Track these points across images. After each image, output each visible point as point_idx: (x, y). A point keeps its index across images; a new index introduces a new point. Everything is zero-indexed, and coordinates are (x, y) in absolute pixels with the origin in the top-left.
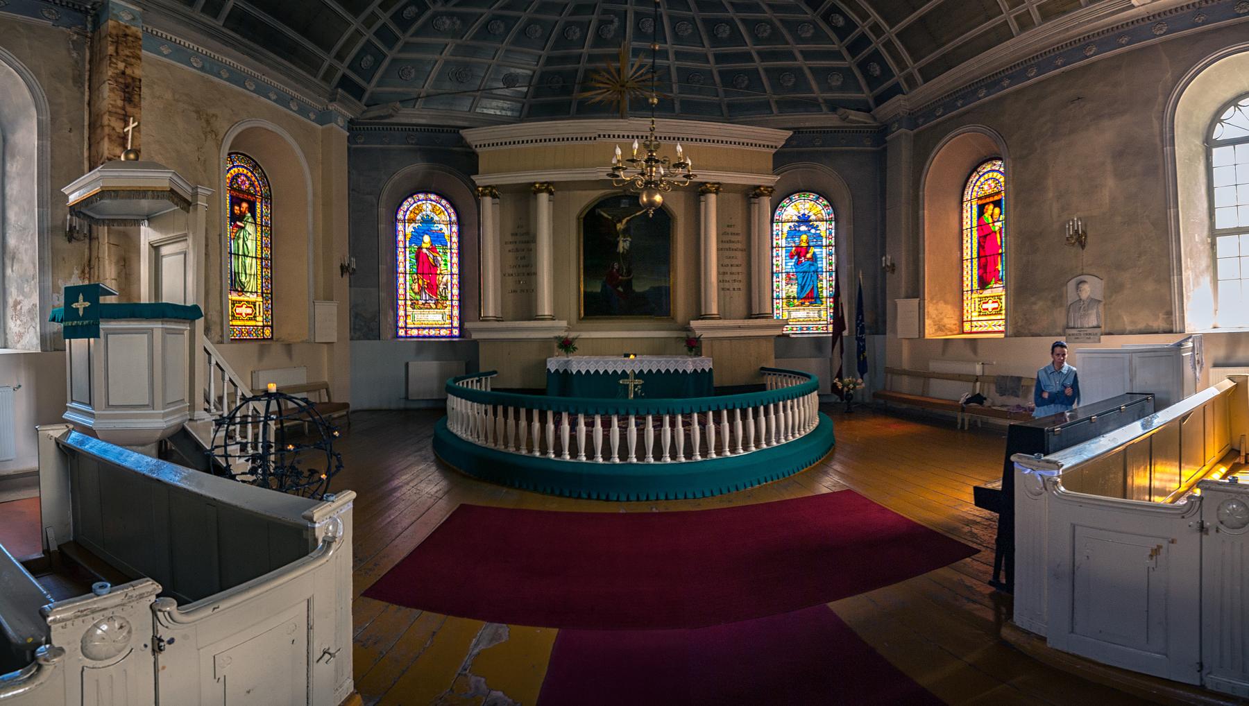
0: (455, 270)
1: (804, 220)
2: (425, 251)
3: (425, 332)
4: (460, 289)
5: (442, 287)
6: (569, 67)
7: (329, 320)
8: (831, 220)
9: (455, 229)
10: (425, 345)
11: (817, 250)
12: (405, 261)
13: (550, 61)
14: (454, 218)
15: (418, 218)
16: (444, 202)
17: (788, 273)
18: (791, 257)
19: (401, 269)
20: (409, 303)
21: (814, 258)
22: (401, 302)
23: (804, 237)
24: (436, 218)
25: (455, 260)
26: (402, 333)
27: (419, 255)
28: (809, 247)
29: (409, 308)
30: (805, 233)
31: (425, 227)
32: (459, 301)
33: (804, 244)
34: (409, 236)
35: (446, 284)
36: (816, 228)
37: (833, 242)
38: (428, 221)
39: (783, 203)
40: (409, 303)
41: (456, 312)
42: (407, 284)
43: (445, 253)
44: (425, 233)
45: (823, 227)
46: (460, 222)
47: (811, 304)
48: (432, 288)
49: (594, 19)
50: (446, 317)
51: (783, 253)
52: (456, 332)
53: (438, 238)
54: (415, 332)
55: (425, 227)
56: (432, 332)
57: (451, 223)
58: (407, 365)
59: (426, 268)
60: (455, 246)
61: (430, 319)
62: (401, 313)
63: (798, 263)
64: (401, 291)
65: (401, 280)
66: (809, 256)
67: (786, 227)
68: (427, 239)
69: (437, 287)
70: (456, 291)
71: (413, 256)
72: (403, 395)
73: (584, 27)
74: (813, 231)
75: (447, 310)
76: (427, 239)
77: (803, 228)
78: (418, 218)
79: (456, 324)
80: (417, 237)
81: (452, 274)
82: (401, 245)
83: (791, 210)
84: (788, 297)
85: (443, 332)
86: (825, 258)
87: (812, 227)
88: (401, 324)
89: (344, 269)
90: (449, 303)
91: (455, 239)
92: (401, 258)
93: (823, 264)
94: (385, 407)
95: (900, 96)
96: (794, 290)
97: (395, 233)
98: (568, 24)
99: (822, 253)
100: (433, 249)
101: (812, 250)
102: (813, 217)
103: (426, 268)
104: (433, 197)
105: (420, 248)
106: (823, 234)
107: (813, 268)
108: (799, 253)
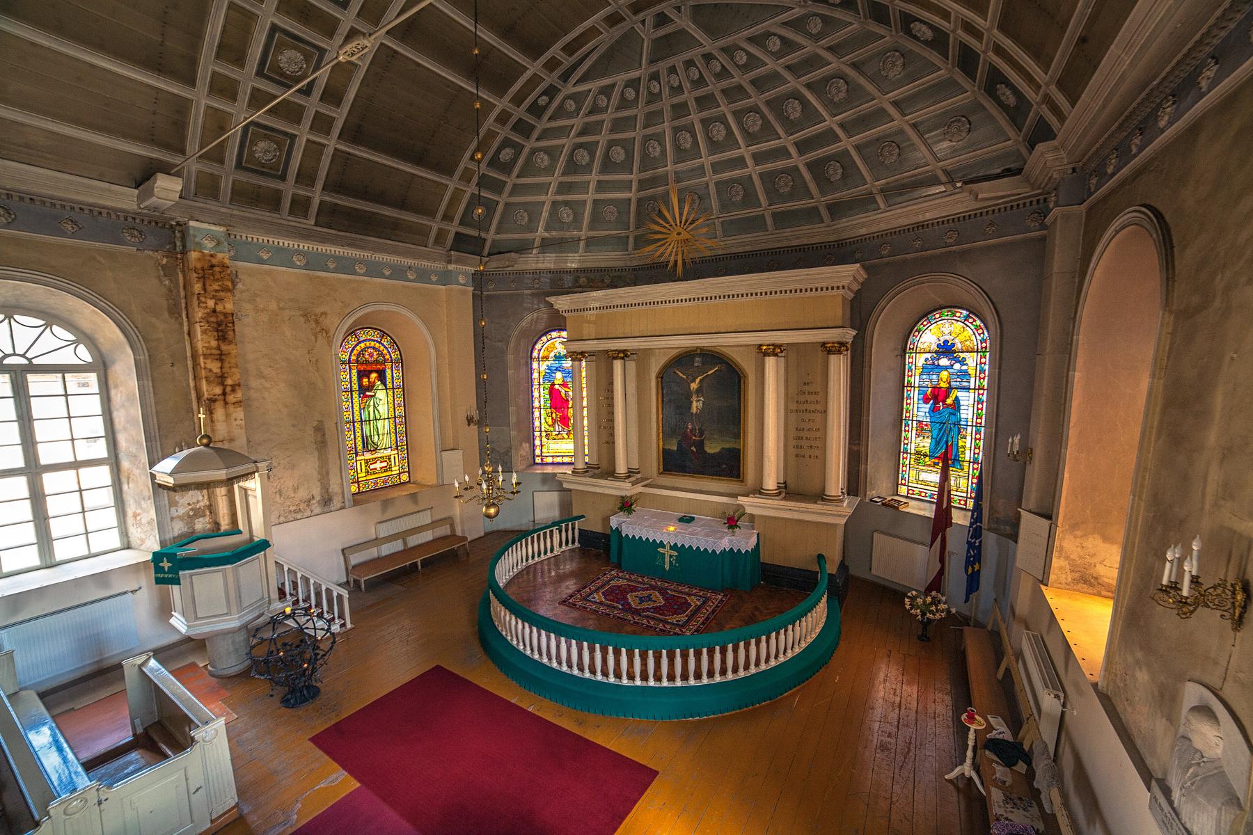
1: (946, 349)
7: (458, 469)
8: (984, 350)
12: (541, 397)
15: (552, 354)
17: (920, 422)
18: (926, 400)
19: (536, 404)
21: (956, 405)
22: (537, 434)
26: (538, 460)
27: (553, 392)
28: (950, 389)
29: (544, 439)
30: (946, 368)
31: (557, 364)
33: (943, 385)
39: (919, 326)
42: (542, 418)
45: (971, 360)
48: (564, 420)
51: (915, 394)
54: (549, 460)
55: (557, 364)
59: (558, 402)
62: (537, 442)
63: (934, 410)
64: (537, 424)
65: (536, 414)
66: (949, 401)
67: (921, 360)
73: (659, 138)
74: (957, 366)
76: (559, 375)
77: (944, 362)
80: (551, 371)
82: (536, 382)
83: (929, 337)
84: (918, 453)
86: (969, 405)
87: (957, 360)
88: (538, 452)
89: (470, 421)
92: (536, 394)
93: (967, 413)
96: (926, 444)
99: (967, 400)
100: (564, 385)
101: (955, 393)
102: (959, 346)
105: (553, 385)
106: (972, 372)
107: (953, 419)
108: (937, 396)
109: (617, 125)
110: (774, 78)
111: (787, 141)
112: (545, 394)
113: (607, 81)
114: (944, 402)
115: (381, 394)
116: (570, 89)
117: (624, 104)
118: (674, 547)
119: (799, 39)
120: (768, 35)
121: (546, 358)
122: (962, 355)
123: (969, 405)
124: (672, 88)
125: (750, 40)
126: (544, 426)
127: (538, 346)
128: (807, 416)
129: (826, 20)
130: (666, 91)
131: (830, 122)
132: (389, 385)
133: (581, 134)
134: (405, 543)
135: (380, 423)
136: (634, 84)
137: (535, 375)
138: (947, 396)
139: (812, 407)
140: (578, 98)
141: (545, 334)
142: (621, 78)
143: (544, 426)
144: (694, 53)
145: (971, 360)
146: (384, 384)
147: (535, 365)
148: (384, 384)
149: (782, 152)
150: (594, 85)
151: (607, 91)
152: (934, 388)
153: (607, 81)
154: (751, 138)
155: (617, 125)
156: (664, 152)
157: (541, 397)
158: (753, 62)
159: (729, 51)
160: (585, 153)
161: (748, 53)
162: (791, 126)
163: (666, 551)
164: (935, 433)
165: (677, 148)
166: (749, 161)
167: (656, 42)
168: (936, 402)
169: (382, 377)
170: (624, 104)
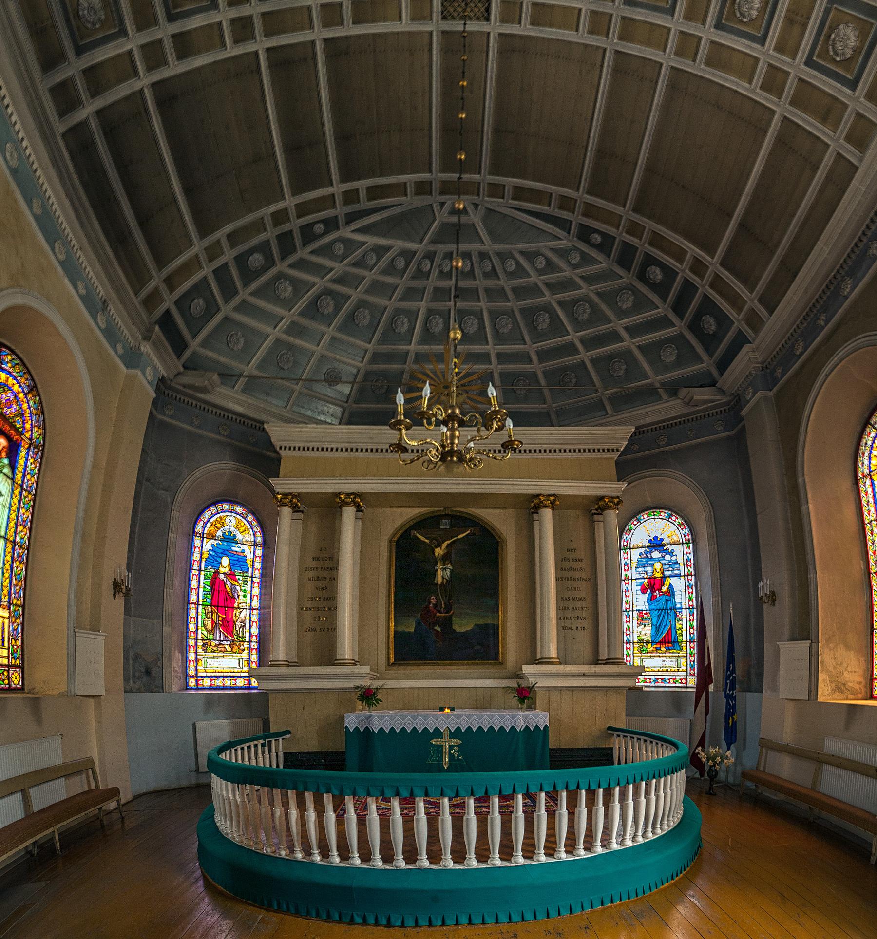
2: (222, 576)
3: (219, 683)
5: (238, 624)
6: (396, 367)
11: (674, 581)
12: (199, 586)
13: (376, 357)
16: (250, 517)
19: (193, 598)
20: (200, 643)
21: (671, 592)
22: (191, 642)
23: (658, 566)
24: (239, 537)
27: (215, 581)
28: (664, 577)
29: (200, 650)
33: (658, 575)
35: (244, 622)
36: (671, 553)
37: (692, 570)
40: (200, 643)
42: (199, 619)
47: (668, 649)
48: (228, 625)
49: (423, 306)
56: (228, 683)
63: (652, 598)
64: (192, 627)
65: (193, 613)
66: (664, 589)
68: (225, 561)
69: (233, 623)
70: (255, 631)
71: (208, 582)
74: (668, 557)
75: (245, 654)
76: (225, 561)
82: (196, 566)
84: (641, 641)
90: (246, 645)
92: (194, 584)
95: (746, 348)
98: (398, 312)
100: (231, 575)
101: (668, 581)
105: (217, 573)
106: (680, 561)
107: (669, 605)
108: (653, 585)
109: (376, 288)
110: (533, 290)
111: (531, 347)
113: (384, 242)
114: (660, 590)
116: (346, 232)
117: (390, 269)
118: (457, 734)
119: (561, 264)
120: (537, 254)
121: (211, 536)
122: (671, 548)
123: (681, 589)
124: (441, 272)
125: (522, 253)
128: (570, 584)
129: (583, 255)
130: (435, 273)
131: (574, 336)
133: (334, 281)
136: (408, 255)
137: (196, 556)
138: (663, 585)
139: (577, 575)
140: (350, 245)
141: (214, 503)
142: (400, 244)
144: (473, 248)
145: (678, 550)
147: (197, 542)
149: (525, 357)
150: (371, 240)
151: (380, 251)
152: (649, 578)
153: (384, 242)
154: (500, 338)
155: (376, 288)
156: (411, 330)
157: (199, 586)
158: (520, 271)
159: (503, 256)
160: (332, 303)
161: (518, 264)
162: (538, 335)
163: (446, 743)
164: (655, 620)
165: (426, 328)
166: (493, 359)
167: (444, 226)
168: (653, 591)
170: (390, 269)
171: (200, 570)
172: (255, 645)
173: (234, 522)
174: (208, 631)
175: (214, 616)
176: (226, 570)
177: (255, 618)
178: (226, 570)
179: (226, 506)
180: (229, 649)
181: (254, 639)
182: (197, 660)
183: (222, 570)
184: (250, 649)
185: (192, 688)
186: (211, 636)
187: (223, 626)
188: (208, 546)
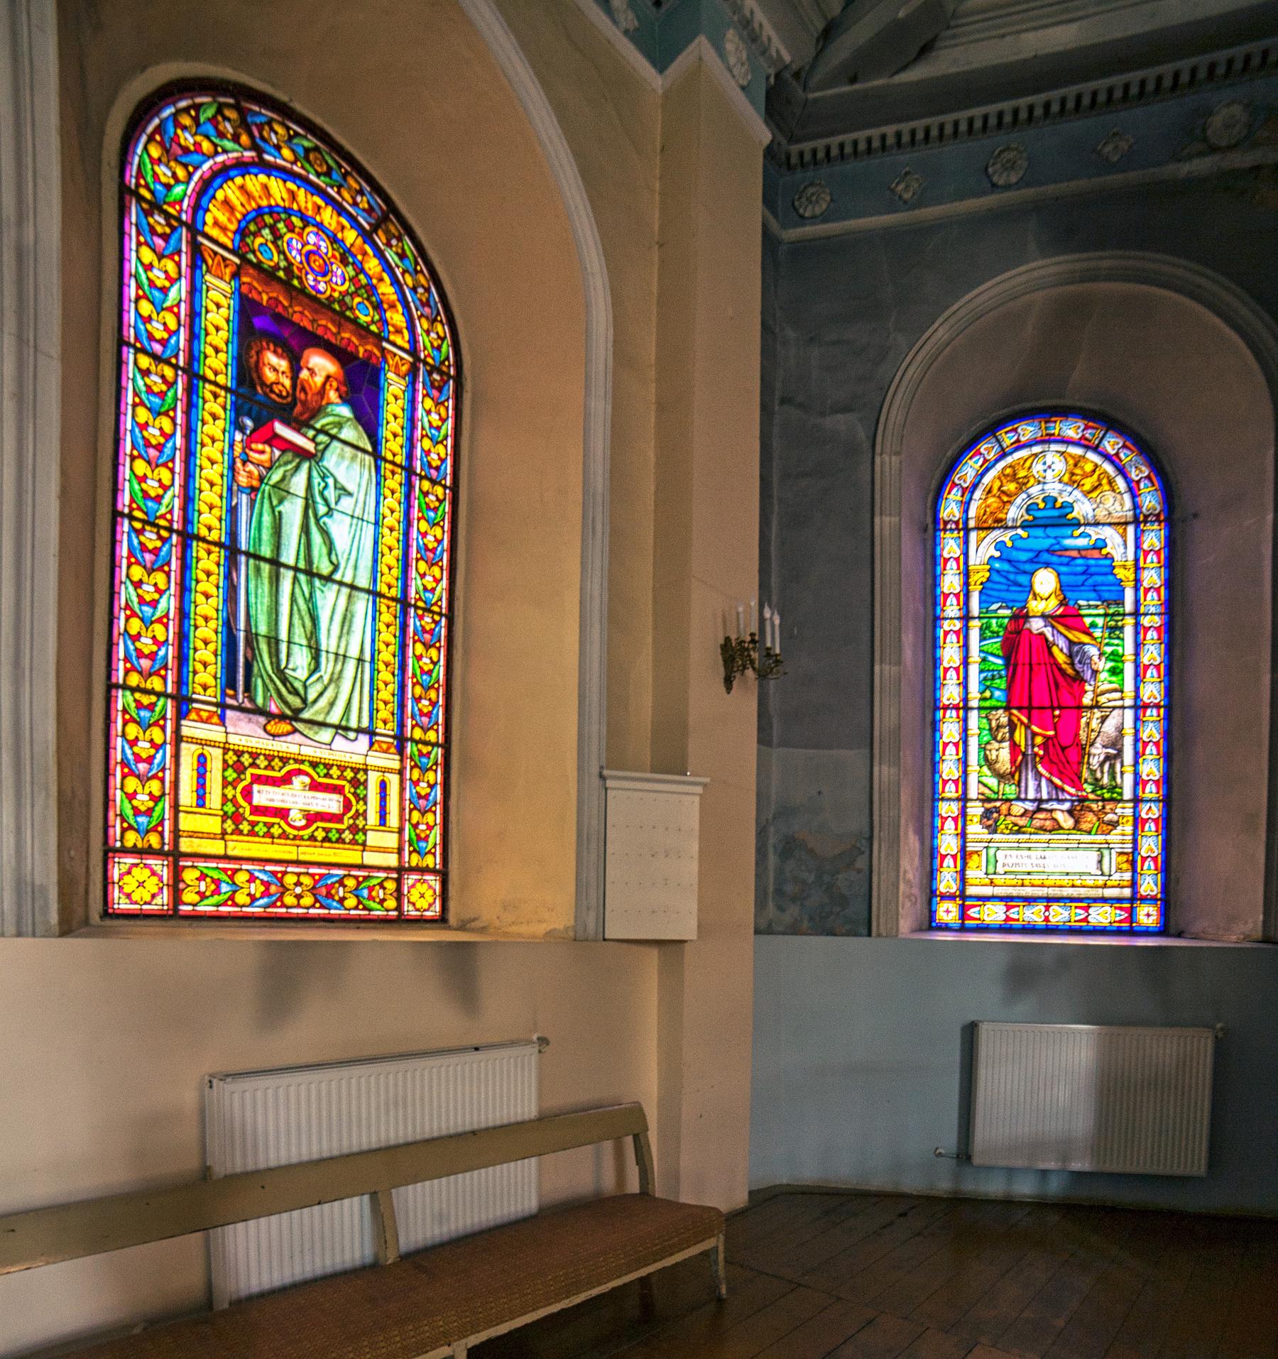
0: (1152, 690)
2: (1036, 625)
3: (1033, 915)
4: (1168, 758)
5: (1098, 752)
9: (1154, 538)
10: (1041, 969)
12: (967, 664)
14: (1150, 500)
15: (1014, 513)
16: (1111, 444)
19: (950, 693)
20: (975, 810)
22: (948, 809)
24: (1083, 509)
25: (1153, 653)
26: (947, 912)
27: (1018, 645)
29: (975, 829)
32: (1167, 801)
34: (978, 578)
35: (1116, 743)
38: (1055, 518)
40: (975, 810)
41: (1150, 844)
42: (973, 745)
43: (1115, 630)
44: (1038, 560)
46: (1171, 516)
48: (1064, 757)
50: (1112, 860)
52: (1147, 916)
53: (1089, 576)
54: (994, 913)
56: (1059, 915)
57: (1138, 520)
58: (970, 1032)
59: (1041, 687)
60: (1152, 602)
61: (1057, 868)
62: (948, 843)
64: (949, 769)
65: (950, 730)
68: (1045, 581)
69: (1081, 751)
70: (1151, 768)
71: (995, 645)
72: (949, 1140)
76: (1045, 581)
78: (1014, 513)
79: (1149, 885)
80: (1010, 577)
81: (1140, 707)
82: (952, 609)
85: (1102, 916)
88: (947, 881)
91: (1153, 576)
92: (950, 654)
94: (878, 1182)
97: (932, 563)
100: (1068, 617)
103: (1041, 687)
104: (1071, 429)
105: (1021, 617)
112: (984, 650)
115: (346, 467)
126: (980, 780)
127: (968, 470)
132: (393, 447)
134: (383, 1220)
135: (329, 600)
137: (951, 582)
143: (980, 780)
146: (369, 420)
147: (950, 546)
148: (369, 420)
157: (967, 664)
169: (361, 387)
171: (966, 618)
172: (1152, 811)
173: (1060, 466)
174: (1001, 777)
175: (1020, 736)
176: (1051, 605)
177: (1152, 732)
178: (1051, 605)
179: (1027, 431)
180: (1067, 822)
181: (1151, 791)
182: (964, 855)
183: (1035, 606)
184: (1138, 822)
185: (946, 928)
186: (1010, 791)
187: (1047, 761)
188: (983, 550)
